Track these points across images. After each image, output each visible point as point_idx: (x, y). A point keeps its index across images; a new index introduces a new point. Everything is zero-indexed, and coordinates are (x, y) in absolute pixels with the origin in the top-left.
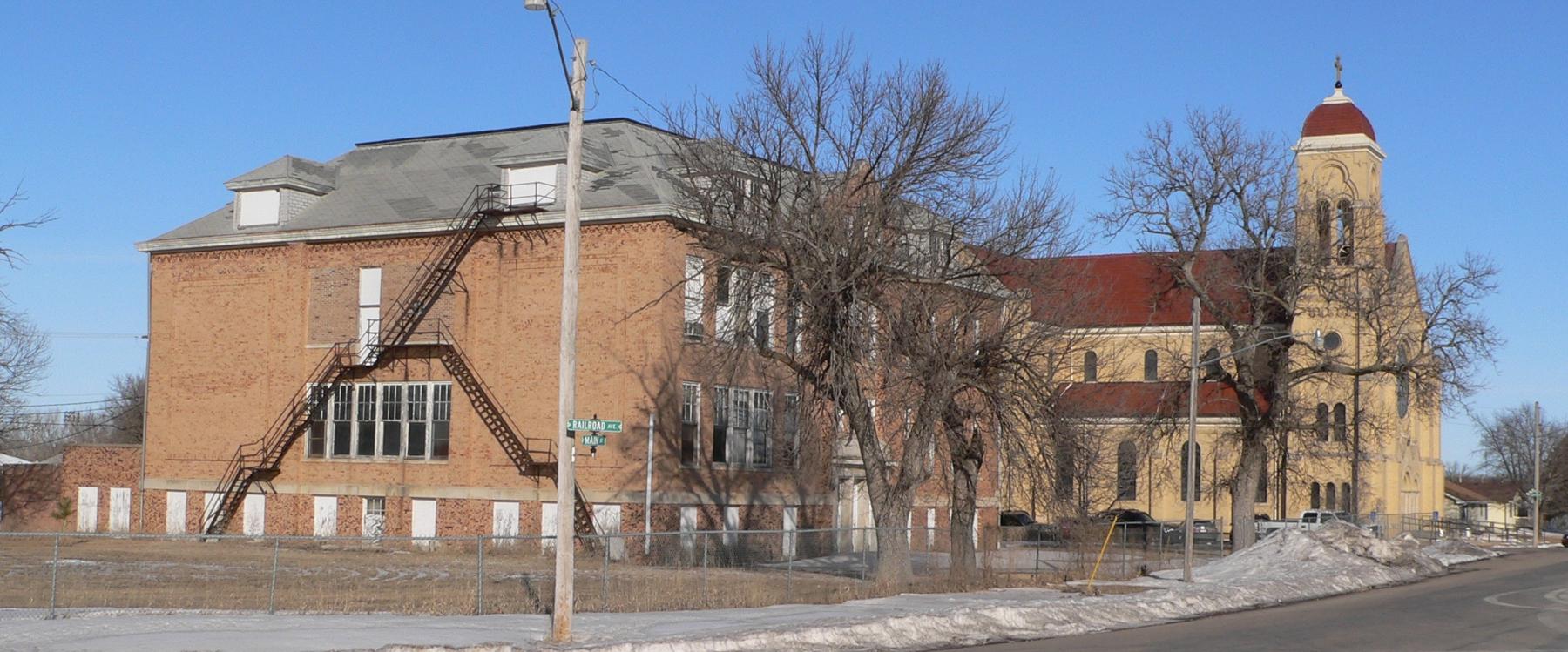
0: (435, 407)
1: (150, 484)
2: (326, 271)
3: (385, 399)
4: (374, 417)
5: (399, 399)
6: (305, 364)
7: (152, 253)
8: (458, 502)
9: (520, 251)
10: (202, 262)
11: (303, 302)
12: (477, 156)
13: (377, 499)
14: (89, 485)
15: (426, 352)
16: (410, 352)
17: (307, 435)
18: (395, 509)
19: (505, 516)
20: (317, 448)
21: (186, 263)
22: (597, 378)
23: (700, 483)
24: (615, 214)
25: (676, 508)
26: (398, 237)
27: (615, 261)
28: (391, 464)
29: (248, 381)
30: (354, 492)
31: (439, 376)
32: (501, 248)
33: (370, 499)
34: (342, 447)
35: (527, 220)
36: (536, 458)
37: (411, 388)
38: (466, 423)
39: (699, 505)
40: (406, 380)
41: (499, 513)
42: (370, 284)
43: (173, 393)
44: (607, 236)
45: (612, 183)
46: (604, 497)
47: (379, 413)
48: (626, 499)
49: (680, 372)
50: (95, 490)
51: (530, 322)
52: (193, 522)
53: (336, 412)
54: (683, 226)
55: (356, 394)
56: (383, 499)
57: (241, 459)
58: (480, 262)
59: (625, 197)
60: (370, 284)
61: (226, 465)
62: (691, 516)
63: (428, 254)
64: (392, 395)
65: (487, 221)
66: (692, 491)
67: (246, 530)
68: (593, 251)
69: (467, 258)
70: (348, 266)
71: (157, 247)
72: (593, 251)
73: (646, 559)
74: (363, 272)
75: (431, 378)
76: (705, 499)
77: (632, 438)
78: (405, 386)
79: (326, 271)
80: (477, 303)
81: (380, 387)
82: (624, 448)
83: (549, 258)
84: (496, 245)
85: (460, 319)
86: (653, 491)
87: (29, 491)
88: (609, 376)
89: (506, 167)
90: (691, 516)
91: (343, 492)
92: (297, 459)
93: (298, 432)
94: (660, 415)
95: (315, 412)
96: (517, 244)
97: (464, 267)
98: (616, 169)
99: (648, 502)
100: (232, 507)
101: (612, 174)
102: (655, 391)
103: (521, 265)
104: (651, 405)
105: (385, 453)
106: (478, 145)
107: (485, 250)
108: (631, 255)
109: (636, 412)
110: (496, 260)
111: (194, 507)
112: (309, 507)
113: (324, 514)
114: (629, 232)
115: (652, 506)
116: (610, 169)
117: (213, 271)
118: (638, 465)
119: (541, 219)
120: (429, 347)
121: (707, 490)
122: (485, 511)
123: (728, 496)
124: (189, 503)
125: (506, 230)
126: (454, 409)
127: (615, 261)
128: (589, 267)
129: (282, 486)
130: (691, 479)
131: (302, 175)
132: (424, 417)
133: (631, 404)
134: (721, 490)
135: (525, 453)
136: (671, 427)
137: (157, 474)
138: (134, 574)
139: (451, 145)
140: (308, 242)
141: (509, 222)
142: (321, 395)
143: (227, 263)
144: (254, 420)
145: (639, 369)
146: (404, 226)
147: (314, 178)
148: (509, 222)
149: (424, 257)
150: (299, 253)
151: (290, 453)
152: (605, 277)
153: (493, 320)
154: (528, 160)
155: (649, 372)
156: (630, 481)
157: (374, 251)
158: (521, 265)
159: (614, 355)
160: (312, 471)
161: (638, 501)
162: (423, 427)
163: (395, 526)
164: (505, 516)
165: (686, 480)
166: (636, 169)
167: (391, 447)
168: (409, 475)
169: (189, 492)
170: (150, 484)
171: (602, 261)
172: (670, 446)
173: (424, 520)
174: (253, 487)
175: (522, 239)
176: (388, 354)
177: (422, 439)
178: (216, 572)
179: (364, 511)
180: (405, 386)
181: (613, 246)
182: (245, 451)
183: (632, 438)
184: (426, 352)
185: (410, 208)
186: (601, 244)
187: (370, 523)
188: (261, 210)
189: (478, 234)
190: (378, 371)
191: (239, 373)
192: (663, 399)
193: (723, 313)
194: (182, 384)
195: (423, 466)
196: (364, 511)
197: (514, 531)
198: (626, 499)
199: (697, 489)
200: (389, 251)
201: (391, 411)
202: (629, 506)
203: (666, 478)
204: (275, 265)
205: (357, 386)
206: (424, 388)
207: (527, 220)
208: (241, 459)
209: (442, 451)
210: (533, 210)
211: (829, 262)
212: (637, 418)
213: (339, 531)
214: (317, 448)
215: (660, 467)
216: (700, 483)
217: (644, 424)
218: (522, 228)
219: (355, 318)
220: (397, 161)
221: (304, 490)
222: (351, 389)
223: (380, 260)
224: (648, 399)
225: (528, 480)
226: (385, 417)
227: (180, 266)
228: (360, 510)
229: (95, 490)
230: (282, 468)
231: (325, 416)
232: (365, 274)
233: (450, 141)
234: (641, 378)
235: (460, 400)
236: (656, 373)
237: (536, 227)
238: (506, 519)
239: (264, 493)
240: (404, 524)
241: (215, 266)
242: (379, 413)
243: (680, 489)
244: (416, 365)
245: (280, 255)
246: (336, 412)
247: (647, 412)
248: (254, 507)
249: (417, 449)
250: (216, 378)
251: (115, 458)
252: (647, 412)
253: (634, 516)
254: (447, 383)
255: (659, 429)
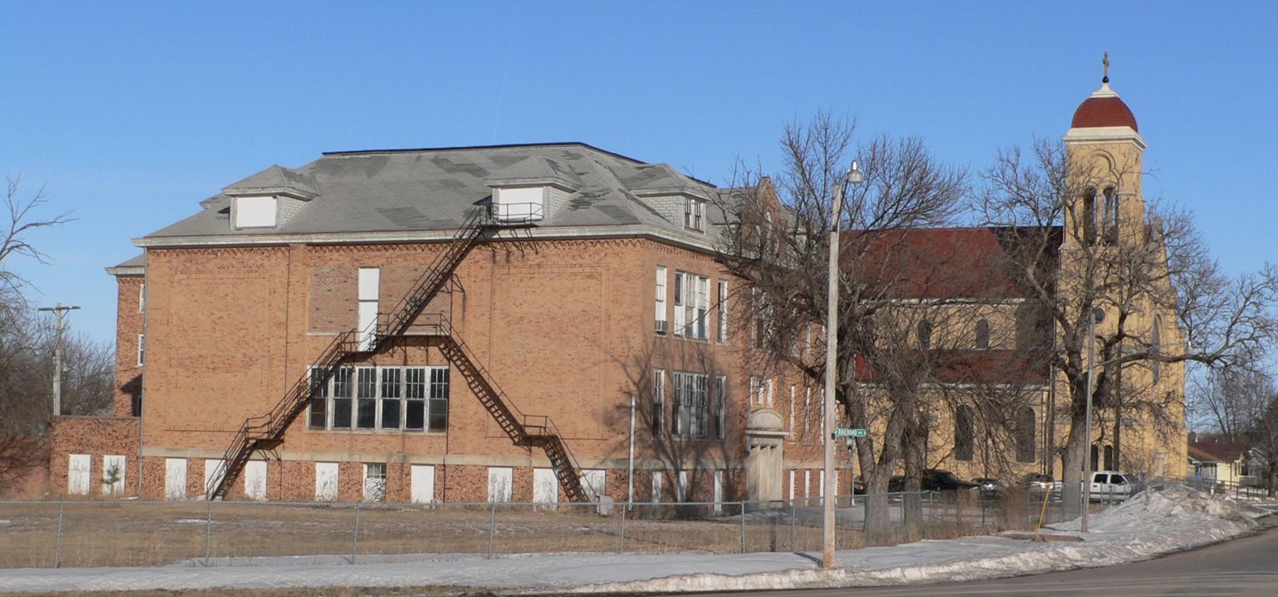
0: (433, 387)
1: (147, 452)
2: (326, 270)
3: (384, 380)
4: (374, 395)
5: (398, 380)
6: (310, 350)
7: (149, 248)
8: (457, 467)
9: (512, 258)
10: (200, 257)
11: (304, 295)
12: (450, 171)
13: (377, 465)
14: (81, 452)
15: (425, 341)
16: (409, 341)
17: (307, 411)
18: (393, 473)
19: (499, 479)
20: (318, 421)
21: (182, 258)
22: (583, 366)
23: (665, 452)
24: (602, 232)
25: (650, 473)
26: (397, 243)
27: (599, 270)
28: (392, 436)
29: (249, 363)
30: (356, 458)
31: (437, 361)
32: (494, 256)
33: (370, 465)
34: (342, 419)
35: (521, 234)
36: (529, 431)
37: (409, 372)
38: (462, 397)
39: (663, 470)
40: (405, 364)
41: (494, 481)
42: (368, 281)
43: (172, 372)
44: (591, 249)
45: (589, 204)
46: (591, 464)
47: (379, 392)
48: (611, 465)
49: (653, 362)
50: (88, 457)
51: (521, 319)
52: (194, 484)
53: (329, 392)
54: (719, 258)
55: (356, 375)
56: (384, 466)
57: (247, 430)
58: (474, 268)
59: (606, 218)
60: (368, 281)
61: (233, 435)
62: (658, 478)
63: (428, 261)
64: (391, 378)
65: (485, 232)
66: (659, 458)
67: (248, 490)
68: (580, 261)
69: (464, 263)
70: (348, 265)
71: (155, 243)
72: (580, 261)
73: (630, 515)
74: (361, 271)
75: (429, 363)
76: (669, 466)
77: (617, 415)
78: (403, 370)
79: (326, 270)
80: (472, 301)
81: (379, 370)
82: (610, 422)
83: (539, 266)
84: (490, 253)
85: (457, 314)
86: (635, 458)
87: (11, 457)
88: (595, 364)
89: (497, 187)
90: (658, 478)
91: (346, 459)
92: (300, 430)
93: (301, 407)
94: (640, 397)
95: (315, 391)
96: (509, 253)
97: (460, 271)
98: (589, 190)
99: (631, 468)
100: (235, 470)
101: (586, 195)
102: (636, 377)
103: (513, 271)
104: (633, 388)
105: (384, 426)
106: (446, 161)
107: (479, 257)
108: (615, 265)
109: (620, 394)
110: (489, 265)
111: (195, 472)
112: (311, 471)
113: (326, 478)
114: (614, 246)
115: (634, 471)
116: (581, 190)
117: (211, 265)
118: (621, 437)
119: (535, 233)
120: (427, 338)
121: (668, 457)
122: (481, 476)
123: (682, 463)
124: (189, 468)
125: (500, 240)
126: (453, 389)
127: (599, 270)
128: (576, 274)
129: (287, 454)
130: (659, 448)
131: (293, 183)
132: (422, 395)
133: (616, 387)
134: (677, 456)
135: (520, 429)
136: (647, 407)
137: (156, 443)
138: (141, 528)
139: (418, 159)
140: (309, 244)
141: (505, 234)
142: (321, 378)
143: (225, 259)
144: (259, 399)
145: (622, 359)
146: (406, 234)
147: (300, 186)
148: (505, 234)
149: (429, 261)
150: (299, 254)
151: (293, 426)
152: (592, 282)
153: (487, 315)
154: (519, 182)
155: (631, 362)
156: (615, 450)
157: (371, 253)
158: (513, 271)
159: (599, 346)
160: (314, 441)
161: (623, 467)
162: (421, 405)
163: (396, 488)
164: (499, 479)
165: (656, 450)
166: (606, 191)
167: (391, 418)
168: (409, 444)
169: (189, 459)
170: (147, 452)
171: (588, 270)
172: (647, 422)
173: (422, 484)
174: (255, 454)
175: (514, 248)
176: (384, 343)
177: (421, 412)
178: (225, 523)
179: (365, 476)
180: (403, 370)
181: (597, 258)
182: (251, 424)
183: (617, 415)
184: (425, 341)
185: (403, 217)
186: (586, 255)
187: (371, 486)
188: (257, 213)
189: (473, 243)
190: (378, 356)
191: (239, 356)
192: (642, 384)
193: (680, 312)
194: (180, 365)
195: (423, 438)
196: (365, 476)
197: (508, 491)
198: (611, 465)
199: (662, 456)
200: (387, 254)
201: (391, 388)
202: (614, 471)
203: (644, 448)
204: (276, 263)
205: (357, 369)
206: (422, 371)
207: (521, 234)
208: (247, 430)
209: (440, 423)
210: (527, 225)
211: (853, 293)
212: (622, 399)
213: (341, 492)
214: (318, 421)
215: (640, 439)
216: (665, 452)
217: (628, 404)
218: (513, 240)
219: (354, 312)
220: (371, 172)
221: (306, 457)
222: (351, 371)
223: (378, 262)
224: (630, 383)
225: (521, 450)
226: (384, 395)
227: (177, 261)
228: (361, 474)
229: (88, 457)
230: (286, 438)
231: (326, 393)
232: (363, 273)
233: (415, 155)
234: (624, 366)
235: (458, 382)
236: (637, 361)
237: (526, 238)
238: (500, 482)
239: (267, 460)
240: (404, 486)
241: (213, 262)
242: (403, 391)
243: (652, 457)
244: (414, 352)
245: (280, 254)
246: (329, 392)
247: (629, 394)
248: (255, 473)
249: (415, 420)
250: (216, 360)
251: (109, 429)
252: (629, 394)
253: (619, 479)
254: (444, 368)
255: (639, 408)
